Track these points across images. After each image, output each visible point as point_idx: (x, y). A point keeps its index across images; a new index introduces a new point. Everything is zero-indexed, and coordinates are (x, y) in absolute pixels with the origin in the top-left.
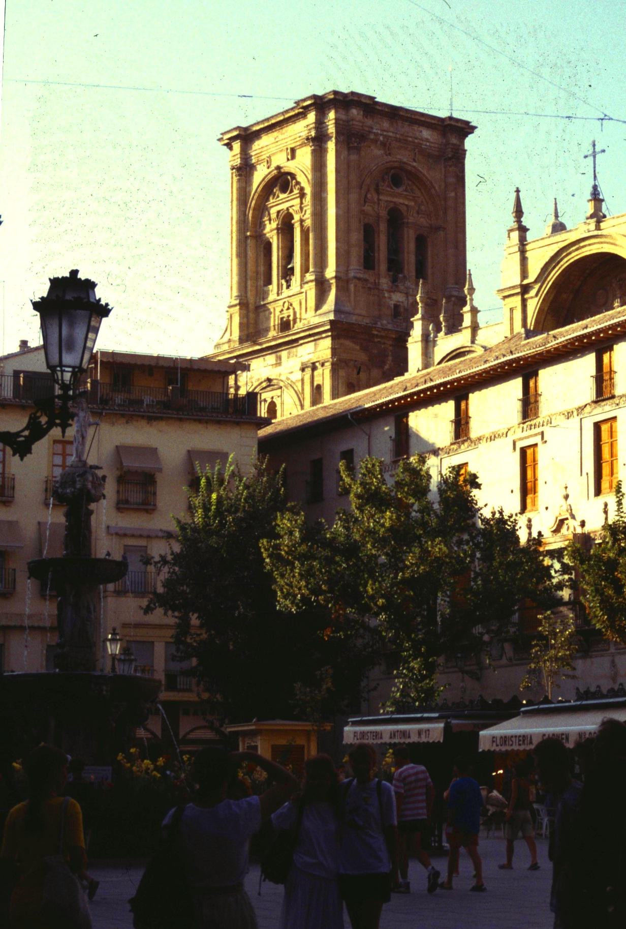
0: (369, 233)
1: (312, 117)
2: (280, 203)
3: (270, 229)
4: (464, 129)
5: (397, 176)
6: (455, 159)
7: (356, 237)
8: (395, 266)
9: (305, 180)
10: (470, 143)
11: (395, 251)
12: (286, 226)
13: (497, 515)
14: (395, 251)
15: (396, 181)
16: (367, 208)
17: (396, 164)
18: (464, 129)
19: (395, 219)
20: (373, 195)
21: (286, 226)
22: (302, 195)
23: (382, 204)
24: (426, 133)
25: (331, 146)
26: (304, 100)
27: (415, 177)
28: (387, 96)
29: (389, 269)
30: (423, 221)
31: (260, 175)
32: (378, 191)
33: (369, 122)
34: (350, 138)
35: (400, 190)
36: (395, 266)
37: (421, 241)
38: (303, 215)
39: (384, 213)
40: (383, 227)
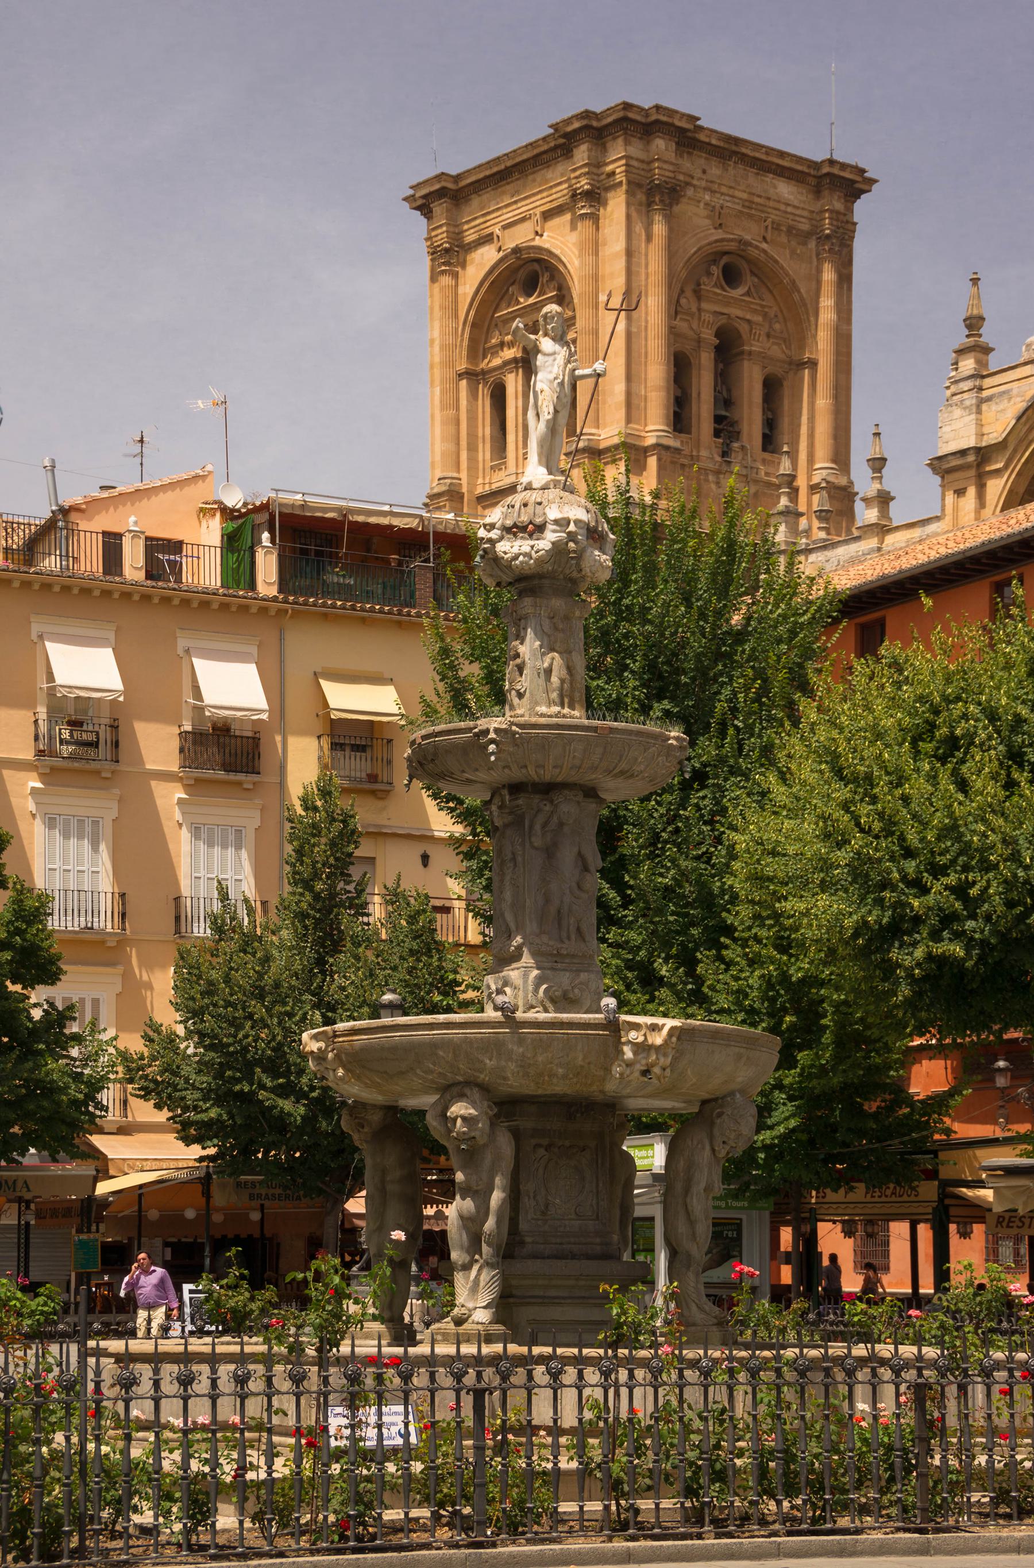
0: (680, 368)
1: (582, 154)
4: (846, 184)
5: (731, 267)
8: (725, 427)
10: (862, 208)
11: (726, 401)
14: (726, 401)
15: (731, 276)
16: (682, 325)
17: (732, 246)
18: (846, 184)
19: (727, 348)
20: (688, 302)
23: (707, 317)
24: (785, 190)
26: (568, 121)
28: (720, 116)
29: (717, 434)
30: (776, 351)
32: (698, 294)
33: (686, 164)
35: (738, 292)
36: (725, 427)
37: (772, 388)
39: (709, 335)
40: (706, 360)
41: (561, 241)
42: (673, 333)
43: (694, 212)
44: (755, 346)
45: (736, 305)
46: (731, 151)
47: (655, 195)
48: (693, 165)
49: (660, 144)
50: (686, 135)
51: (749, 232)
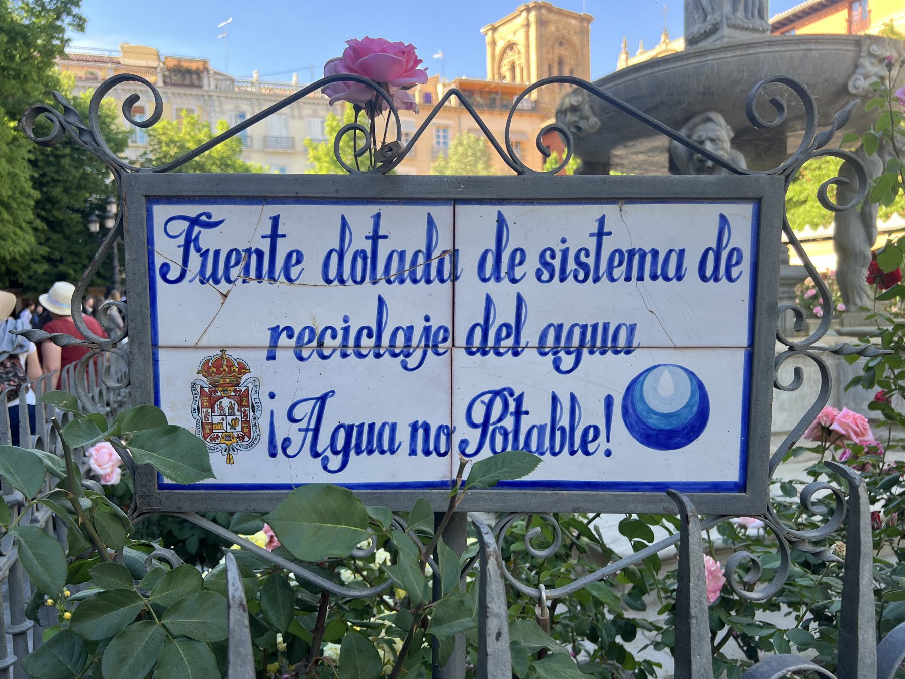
1: (524, 14)
2: (510, 57)
4: (587, 19)
9: (522, 47)
12: (513, 68)
15: (561, 44)
21: (513, 68)
22: (519, 52)
24: (573, 22)
27: (570, 43)
34: (542, 23)
38: (521, 61)
39: (556, 60)
41: (520, 39)
43: (552, 28)
45: (563, 52)
46: (559, 12)
48: (552, 17)
50: (550, 9)
51: (565, 32)
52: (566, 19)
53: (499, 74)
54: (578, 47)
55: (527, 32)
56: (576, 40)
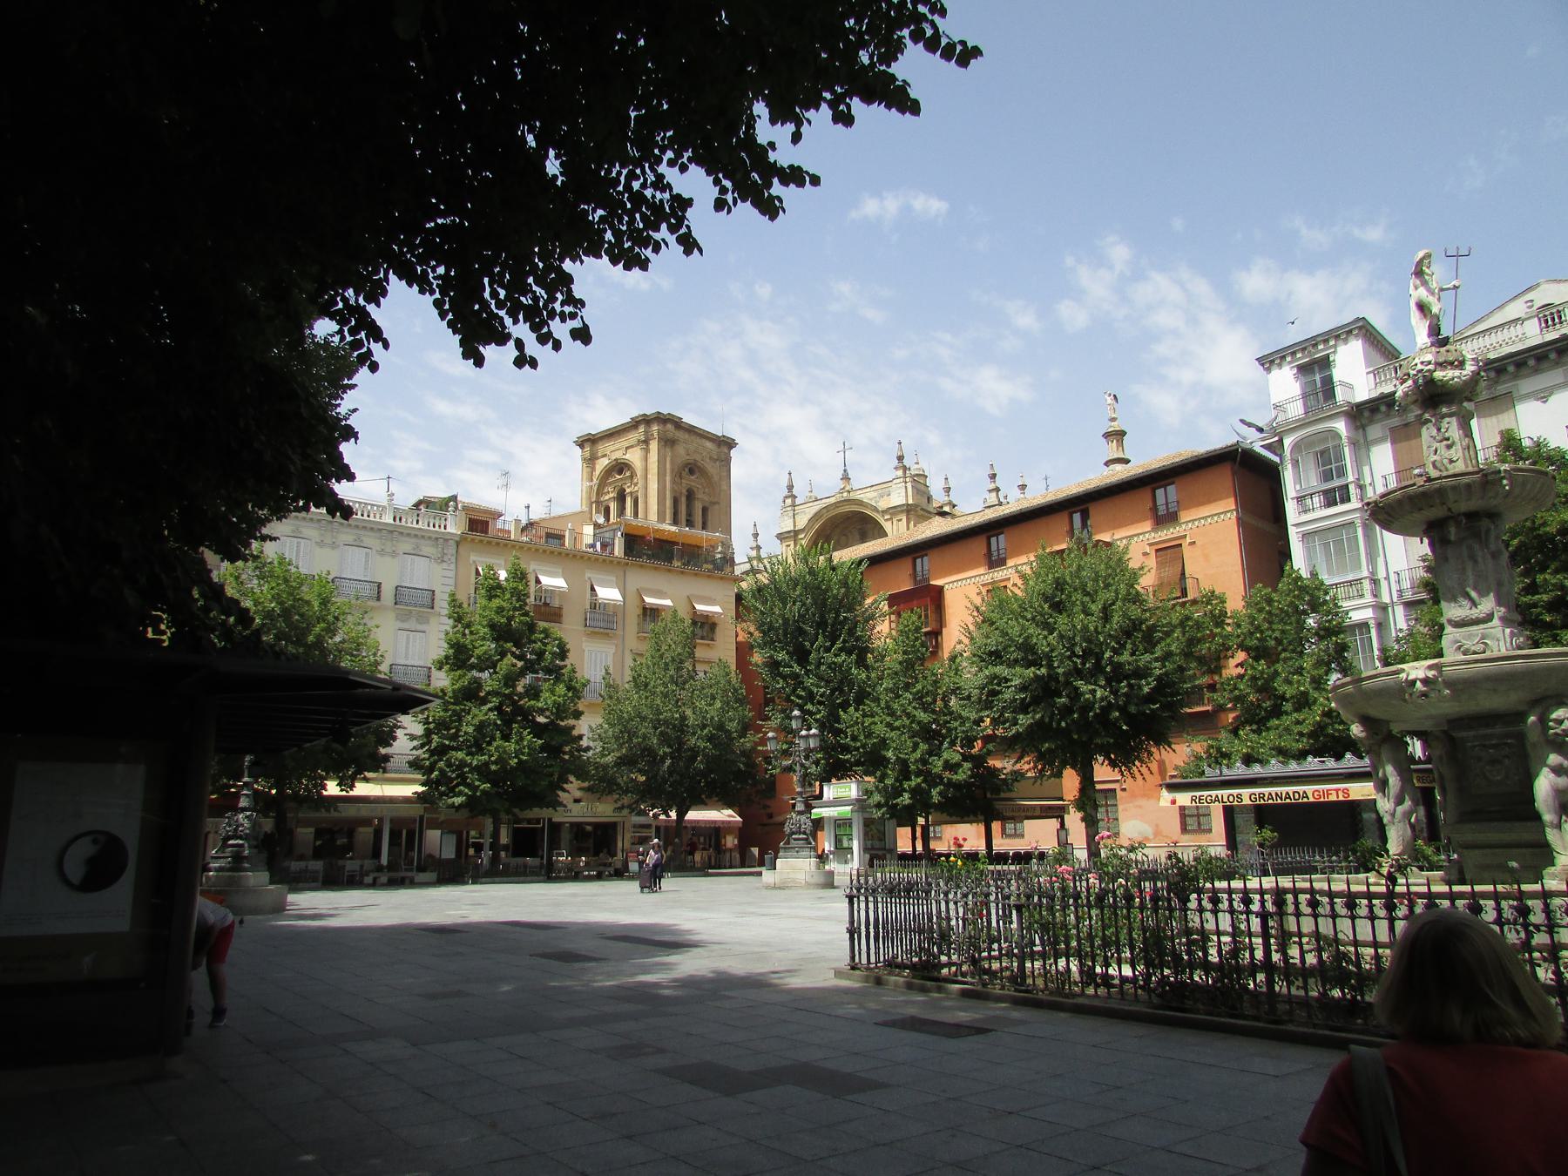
0: (676, 501)
1: (642, 429)
3: (610, 494)
4: (728, 444)
5: (692, 468)
6: (727, 461)
7: (669, 503)
10: (733, 452)
11: (689, 514)
13: (984, 591)
14: (689, 514)
15: (691, 472)
19: (690, 496)
24: (709, 444)
25: (654, 446)
28: (689, 419)
31: (602, 464)
37: (705, 510)
40: (684, 499)
41: (634, 457)
42: (673, 490)
43: (681, 450)
44: (700, 495)
45: (692, 481)
46: (692, 430)
47: (667, 442)
48: (680, 435)
49: (669, 426)
50: (678, 423)
51: (698, 458)
52: (698, 440)
53: (598, 502)
54: (716, 478)
55: (647, 451)
56: (712, 468)
